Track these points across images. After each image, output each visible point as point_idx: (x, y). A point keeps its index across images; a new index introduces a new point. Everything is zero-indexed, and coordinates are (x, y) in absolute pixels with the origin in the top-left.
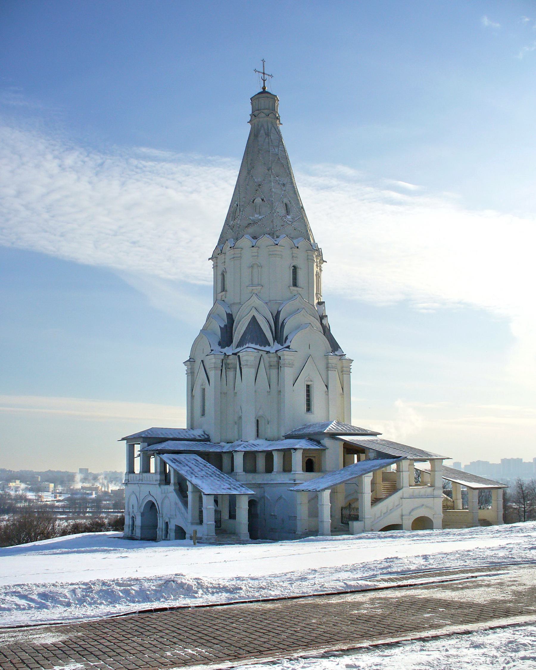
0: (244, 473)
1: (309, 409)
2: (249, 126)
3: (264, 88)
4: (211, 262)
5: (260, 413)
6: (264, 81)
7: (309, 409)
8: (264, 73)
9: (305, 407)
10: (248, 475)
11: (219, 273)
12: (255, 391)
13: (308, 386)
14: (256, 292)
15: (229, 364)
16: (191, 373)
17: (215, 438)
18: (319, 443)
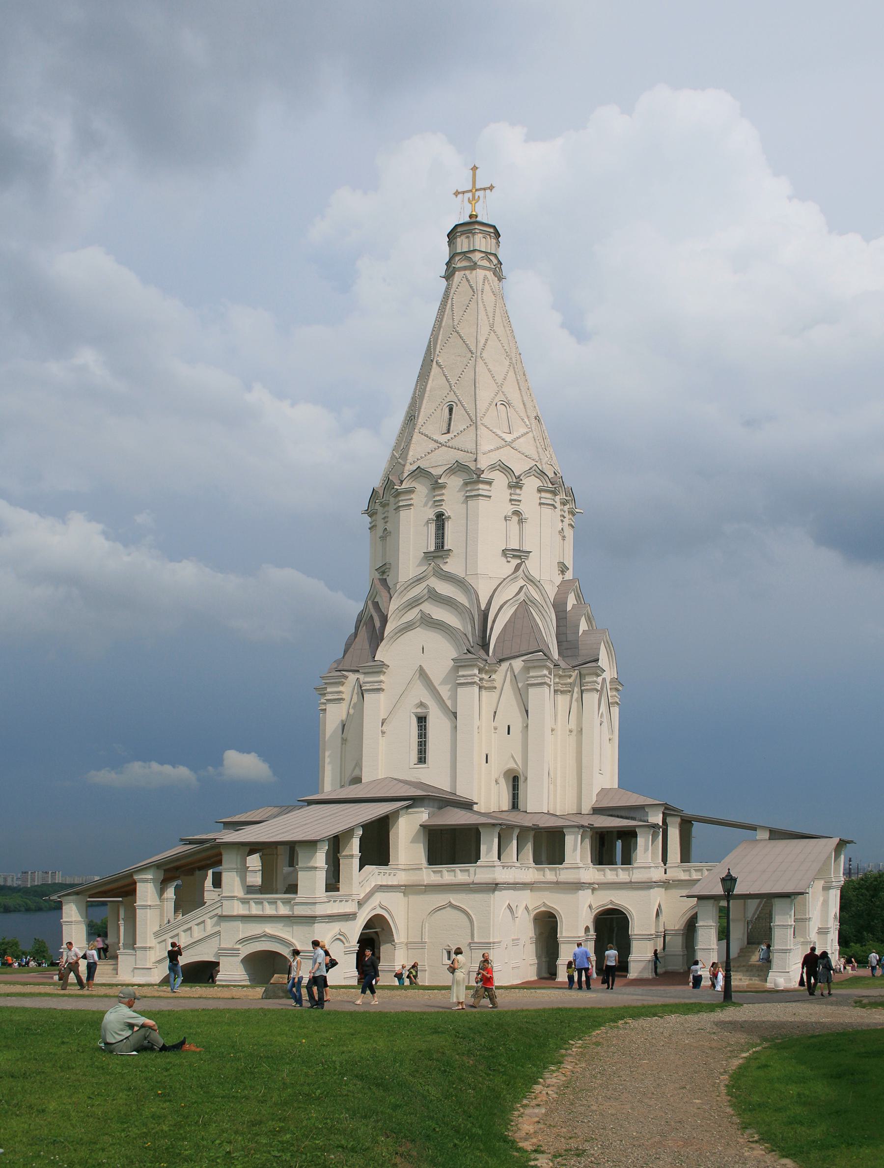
3: (471, 216)
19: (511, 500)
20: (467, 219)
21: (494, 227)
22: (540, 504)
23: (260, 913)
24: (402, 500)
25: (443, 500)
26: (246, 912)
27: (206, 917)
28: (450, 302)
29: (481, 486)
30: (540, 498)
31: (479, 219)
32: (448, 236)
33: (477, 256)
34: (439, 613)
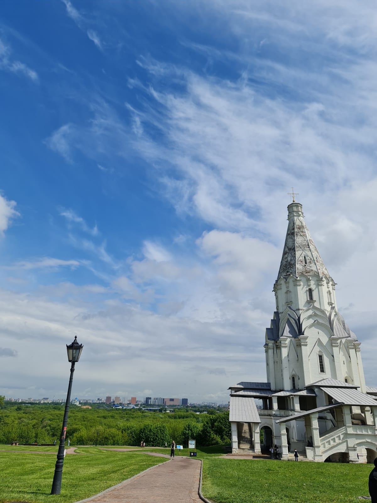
0: (278, 410)
1: (322, 370)
2: (288, 221)
3: (294, 201)
4: (274, 292)
5: (294, 373)
6: (293, 197)
7: (322, 370)
8: (293, 194)
9: (319, 369)
10: (281, 411)
11: (276, 297)
12: (288, 360)
13: (321, 357)
14: (289, 305)
15: (277, 346)
16: (267, 352)
17: (273, 388)
18: (314, 392)
19: (328, 287)
20: (293, 202)
21: (302, 205)
22: (333, 289)
23: (361, 433)
24: (298, 283)
25: (310, 285)
26: (355, 433)
27: (340, 434)
28: (295, 225)
29: (322, 282)
30: (332, 287)
31: (296, 202)
32: (289, 206)
33: (300, 213)
34: (320, 321)
